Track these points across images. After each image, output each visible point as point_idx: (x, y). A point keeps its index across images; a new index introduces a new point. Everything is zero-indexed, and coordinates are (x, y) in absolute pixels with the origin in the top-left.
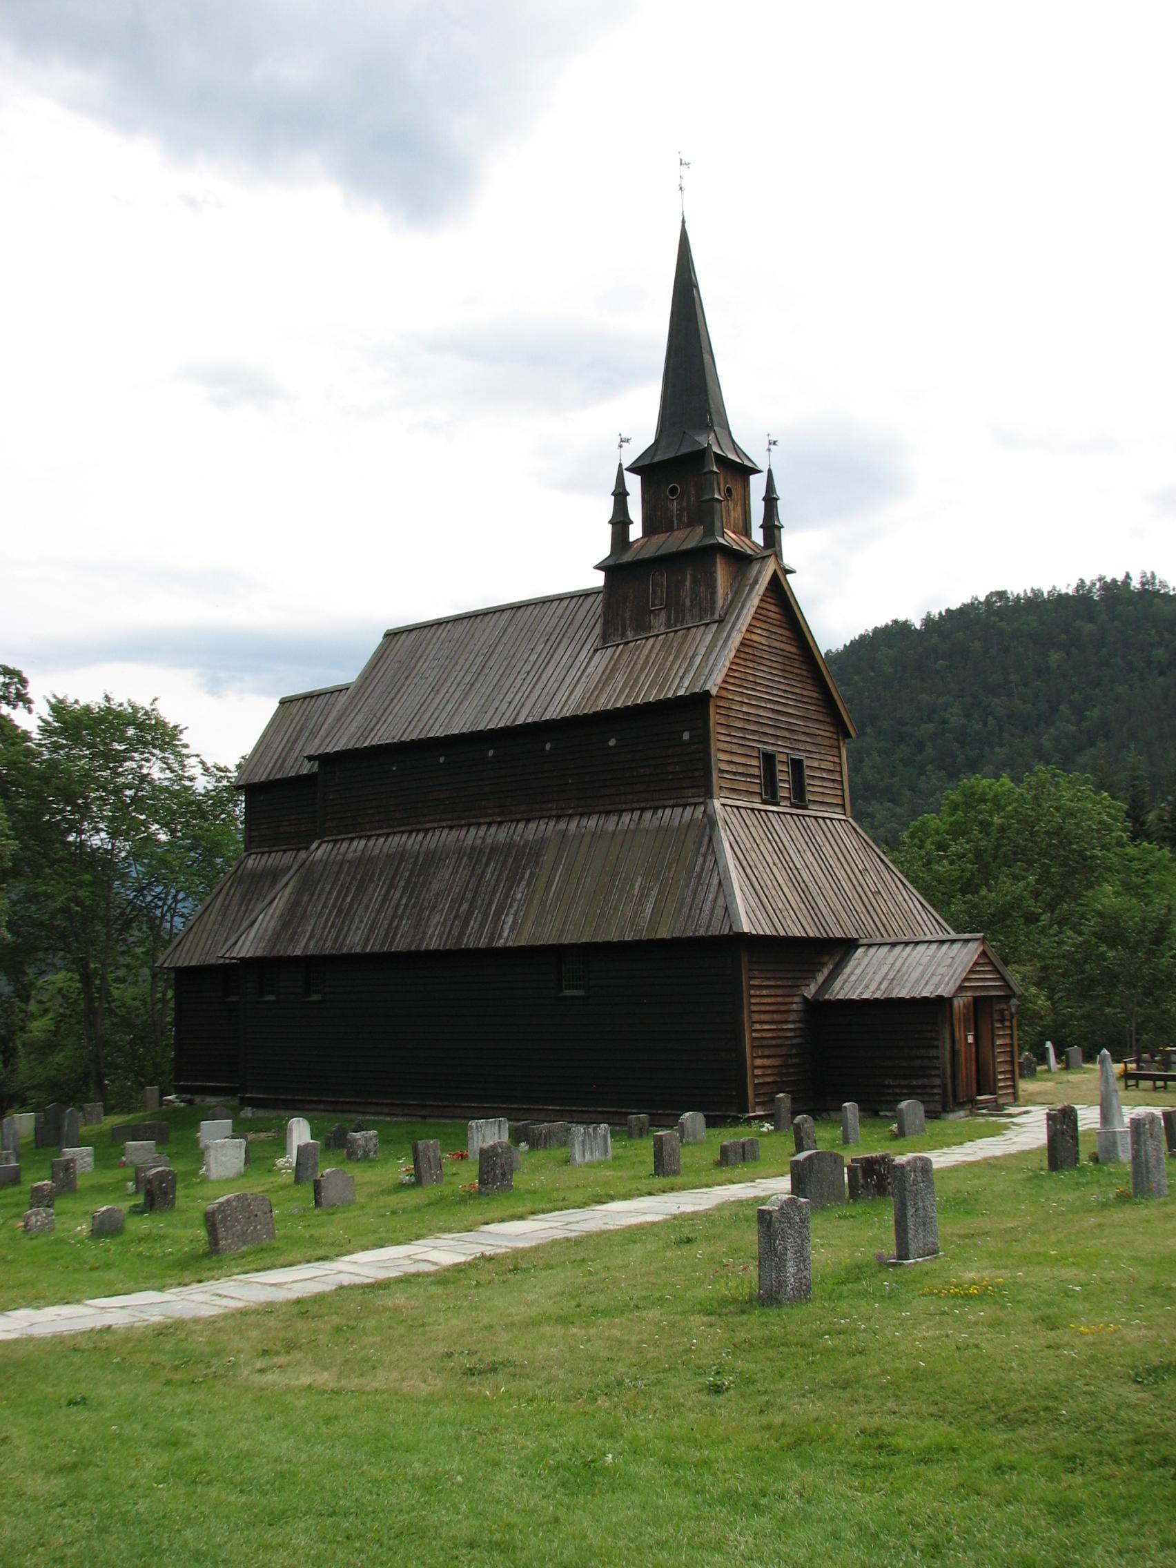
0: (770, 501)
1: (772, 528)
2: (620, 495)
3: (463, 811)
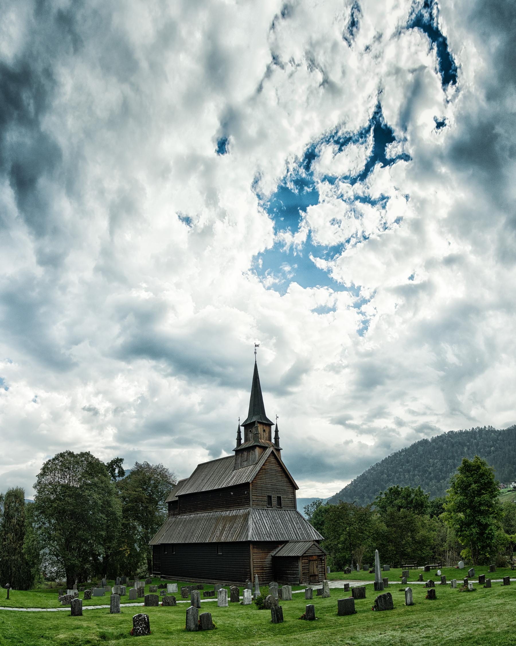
0: (277, 431)
1: (277, 438)
2: (239, 432)
3: (204, 509)
